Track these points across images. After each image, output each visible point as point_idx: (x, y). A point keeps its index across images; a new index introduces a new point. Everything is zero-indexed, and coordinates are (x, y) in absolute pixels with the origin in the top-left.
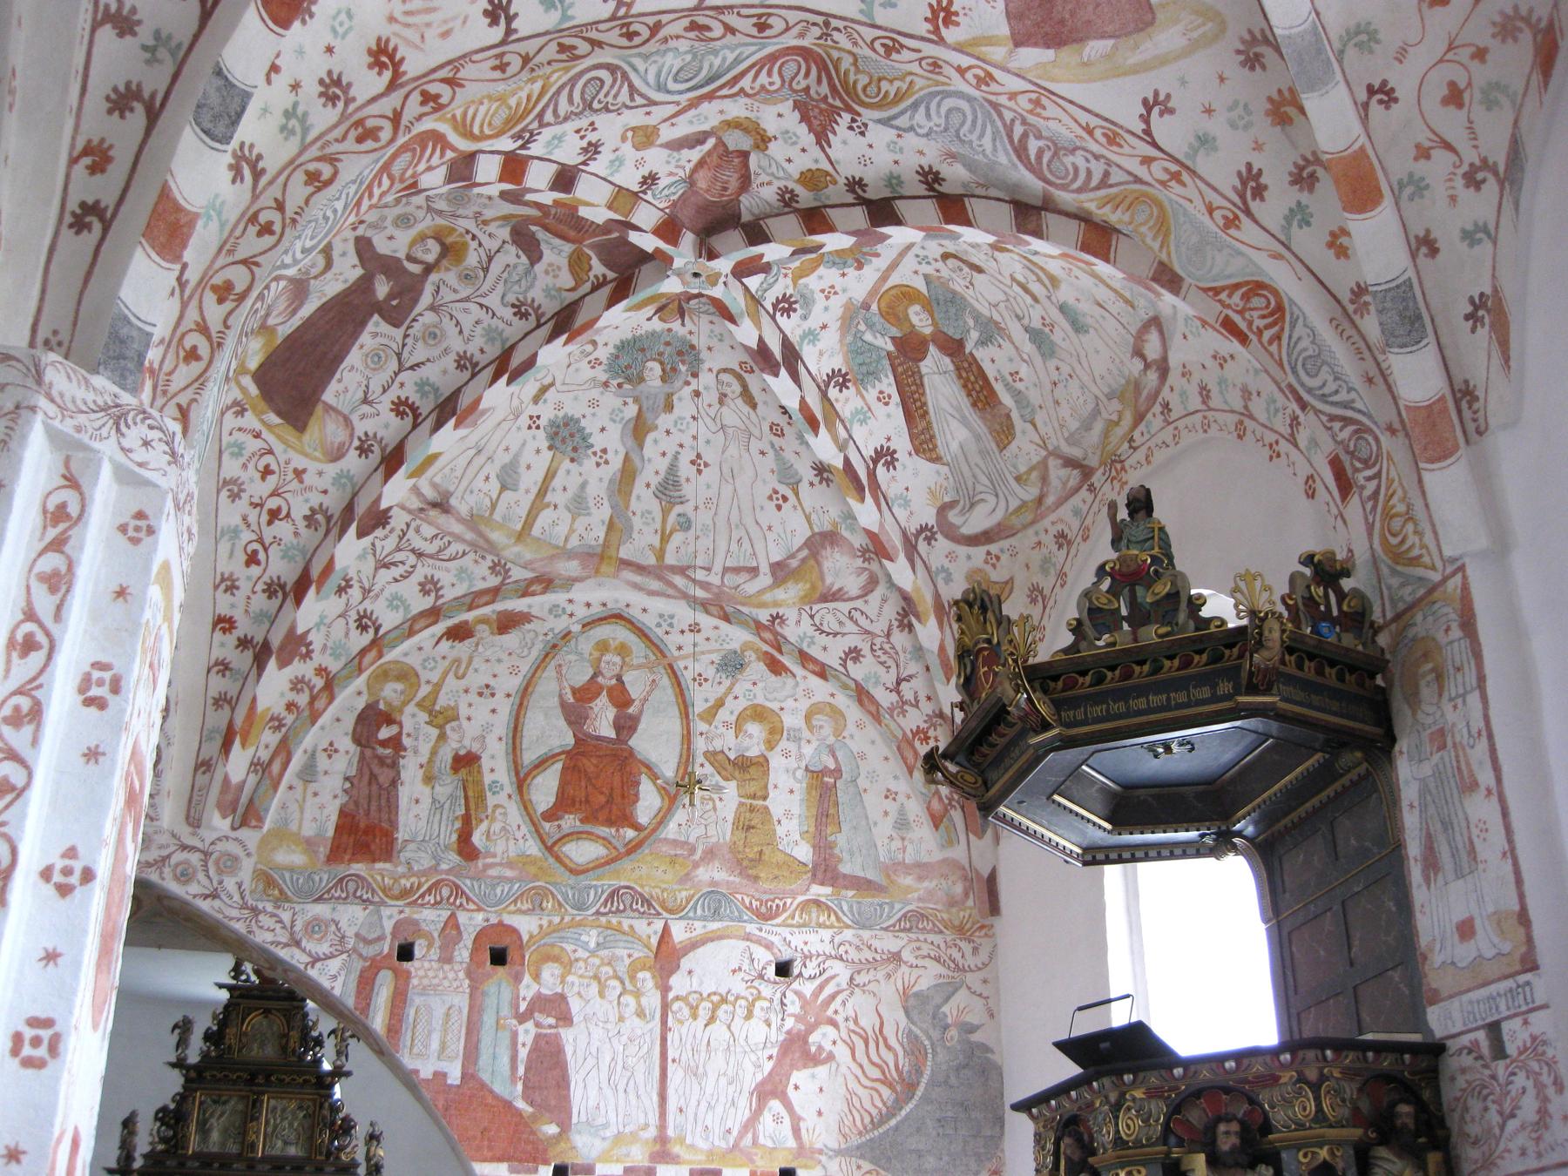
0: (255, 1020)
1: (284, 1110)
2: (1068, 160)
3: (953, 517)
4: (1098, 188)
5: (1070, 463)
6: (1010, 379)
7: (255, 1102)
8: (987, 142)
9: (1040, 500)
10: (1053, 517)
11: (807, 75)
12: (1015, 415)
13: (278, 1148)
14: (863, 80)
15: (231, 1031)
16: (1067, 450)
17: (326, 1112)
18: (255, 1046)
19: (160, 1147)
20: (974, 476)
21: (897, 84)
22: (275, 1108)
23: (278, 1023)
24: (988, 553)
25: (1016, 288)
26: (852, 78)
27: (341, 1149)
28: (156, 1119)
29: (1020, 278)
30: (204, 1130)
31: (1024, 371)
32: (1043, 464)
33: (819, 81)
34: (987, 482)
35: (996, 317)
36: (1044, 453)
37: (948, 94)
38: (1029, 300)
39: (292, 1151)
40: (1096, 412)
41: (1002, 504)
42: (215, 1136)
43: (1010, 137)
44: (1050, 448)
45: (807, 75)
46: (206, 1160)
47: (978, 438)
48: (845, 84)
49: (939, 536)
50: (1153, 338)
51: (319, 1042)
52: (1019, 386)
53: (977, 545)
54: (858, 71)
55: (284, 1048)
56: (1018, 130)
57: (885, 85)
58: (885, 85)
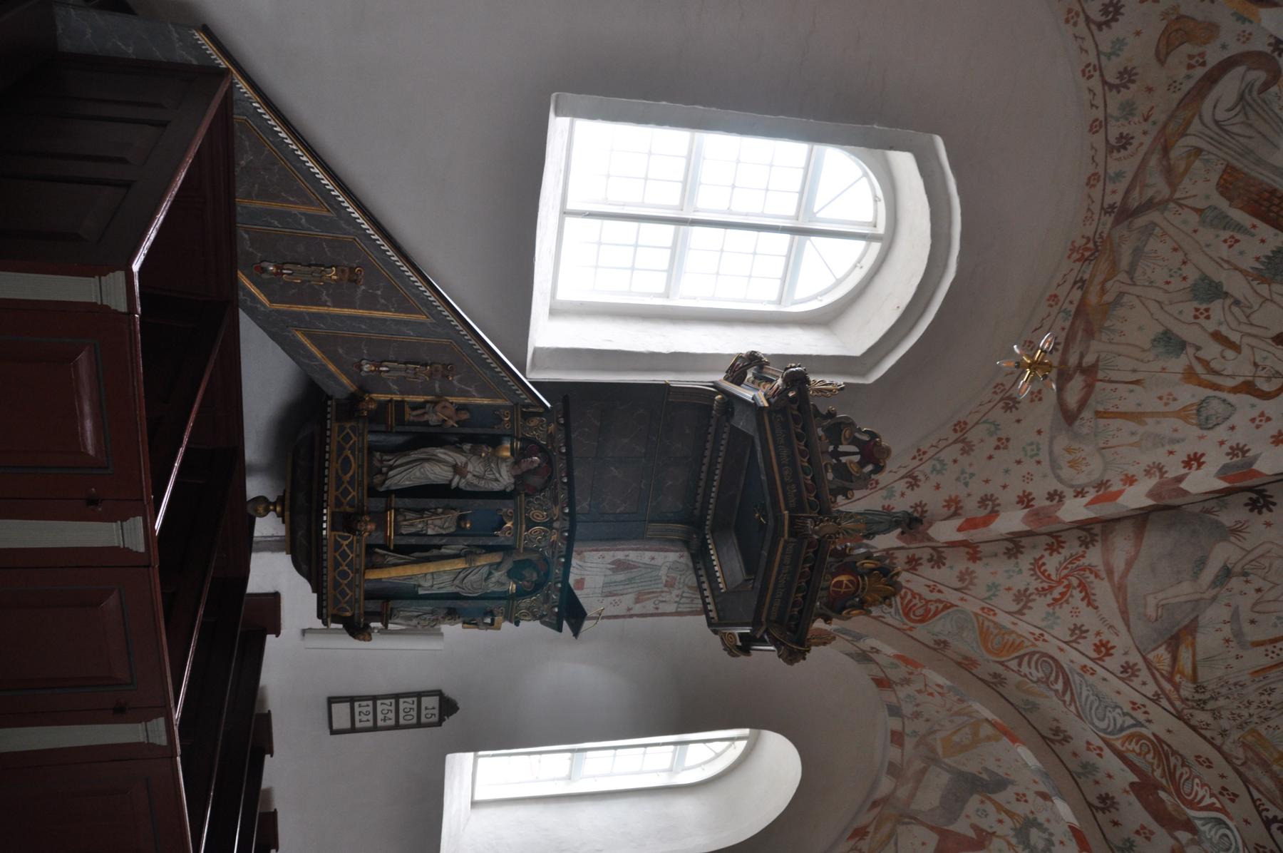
2: (1041, 674)
3: (1260, 76)
4: (1024, 655)
5: (1149, 205)
6: (1238, 236)
8: (1085, 694)
9: (1166, 151)
10: (1144, 148)
11: (1182, 775)
12: (1223, 204)
14: (1150, 756)
16: (1154, 216)
20: (1250, 126)
21: (1130, 748)
24: (1203, 64)
25: (1234, 337)
26: (1156, 762)
29: (1230, 354)
31: (1224, 251)
32: (1173, 186)
33: (1175, 766)
34: (1235, 129)
35: (1263, 289)
36: (1177, 195)
37: (1104, 731)
38: (1224, 330)
40: (1131, 272)
41: (1207, 118)
43: (1072, 694)
44: (1172, 205)
45: (1182, 775)
47: (1259, 162)
48: (1160, 760)
49: (1269, 50)
50: (1072, 399)
52: (1226, 234)
53: (1220, 63)
54: (1152, 764)
56: (1067, 697)
57: (1137, 749)
58: (1137, 749)
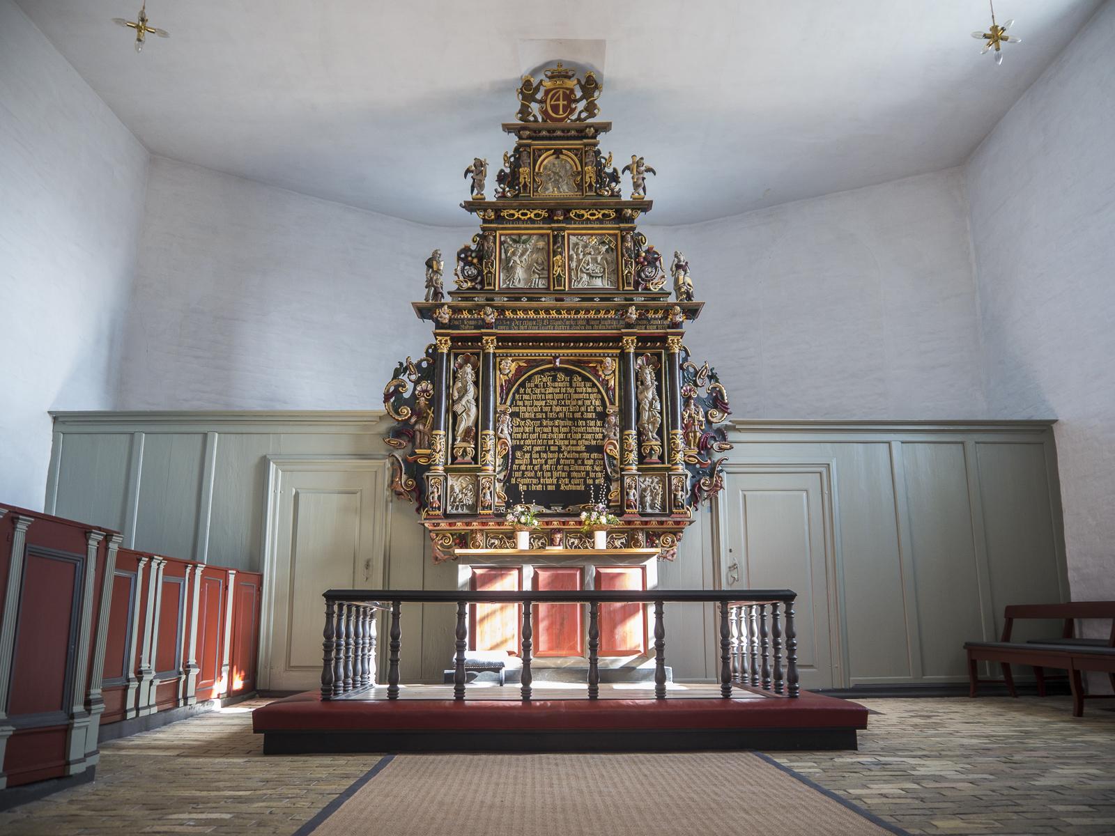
0: (547, 160)
1: (585, 247)
7: (555, 237)
13: (584, 282)
15: (524, 170)
17: (629, 244)
18: (550, 186)
19: (465, 286)
22: (577, 244)
23: (570, 160)
27: (649, 279)
28: (459, 258)
30: (509, 269)
39: (598, 283)
42: (520, 273)
46: (515, 295)
51: (615, 177)
55: (580, 186)
